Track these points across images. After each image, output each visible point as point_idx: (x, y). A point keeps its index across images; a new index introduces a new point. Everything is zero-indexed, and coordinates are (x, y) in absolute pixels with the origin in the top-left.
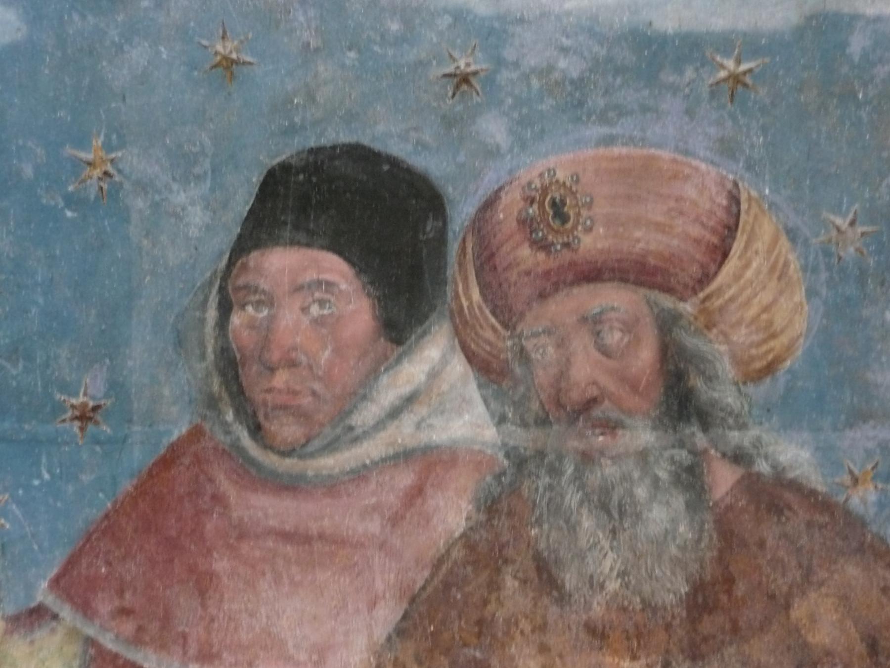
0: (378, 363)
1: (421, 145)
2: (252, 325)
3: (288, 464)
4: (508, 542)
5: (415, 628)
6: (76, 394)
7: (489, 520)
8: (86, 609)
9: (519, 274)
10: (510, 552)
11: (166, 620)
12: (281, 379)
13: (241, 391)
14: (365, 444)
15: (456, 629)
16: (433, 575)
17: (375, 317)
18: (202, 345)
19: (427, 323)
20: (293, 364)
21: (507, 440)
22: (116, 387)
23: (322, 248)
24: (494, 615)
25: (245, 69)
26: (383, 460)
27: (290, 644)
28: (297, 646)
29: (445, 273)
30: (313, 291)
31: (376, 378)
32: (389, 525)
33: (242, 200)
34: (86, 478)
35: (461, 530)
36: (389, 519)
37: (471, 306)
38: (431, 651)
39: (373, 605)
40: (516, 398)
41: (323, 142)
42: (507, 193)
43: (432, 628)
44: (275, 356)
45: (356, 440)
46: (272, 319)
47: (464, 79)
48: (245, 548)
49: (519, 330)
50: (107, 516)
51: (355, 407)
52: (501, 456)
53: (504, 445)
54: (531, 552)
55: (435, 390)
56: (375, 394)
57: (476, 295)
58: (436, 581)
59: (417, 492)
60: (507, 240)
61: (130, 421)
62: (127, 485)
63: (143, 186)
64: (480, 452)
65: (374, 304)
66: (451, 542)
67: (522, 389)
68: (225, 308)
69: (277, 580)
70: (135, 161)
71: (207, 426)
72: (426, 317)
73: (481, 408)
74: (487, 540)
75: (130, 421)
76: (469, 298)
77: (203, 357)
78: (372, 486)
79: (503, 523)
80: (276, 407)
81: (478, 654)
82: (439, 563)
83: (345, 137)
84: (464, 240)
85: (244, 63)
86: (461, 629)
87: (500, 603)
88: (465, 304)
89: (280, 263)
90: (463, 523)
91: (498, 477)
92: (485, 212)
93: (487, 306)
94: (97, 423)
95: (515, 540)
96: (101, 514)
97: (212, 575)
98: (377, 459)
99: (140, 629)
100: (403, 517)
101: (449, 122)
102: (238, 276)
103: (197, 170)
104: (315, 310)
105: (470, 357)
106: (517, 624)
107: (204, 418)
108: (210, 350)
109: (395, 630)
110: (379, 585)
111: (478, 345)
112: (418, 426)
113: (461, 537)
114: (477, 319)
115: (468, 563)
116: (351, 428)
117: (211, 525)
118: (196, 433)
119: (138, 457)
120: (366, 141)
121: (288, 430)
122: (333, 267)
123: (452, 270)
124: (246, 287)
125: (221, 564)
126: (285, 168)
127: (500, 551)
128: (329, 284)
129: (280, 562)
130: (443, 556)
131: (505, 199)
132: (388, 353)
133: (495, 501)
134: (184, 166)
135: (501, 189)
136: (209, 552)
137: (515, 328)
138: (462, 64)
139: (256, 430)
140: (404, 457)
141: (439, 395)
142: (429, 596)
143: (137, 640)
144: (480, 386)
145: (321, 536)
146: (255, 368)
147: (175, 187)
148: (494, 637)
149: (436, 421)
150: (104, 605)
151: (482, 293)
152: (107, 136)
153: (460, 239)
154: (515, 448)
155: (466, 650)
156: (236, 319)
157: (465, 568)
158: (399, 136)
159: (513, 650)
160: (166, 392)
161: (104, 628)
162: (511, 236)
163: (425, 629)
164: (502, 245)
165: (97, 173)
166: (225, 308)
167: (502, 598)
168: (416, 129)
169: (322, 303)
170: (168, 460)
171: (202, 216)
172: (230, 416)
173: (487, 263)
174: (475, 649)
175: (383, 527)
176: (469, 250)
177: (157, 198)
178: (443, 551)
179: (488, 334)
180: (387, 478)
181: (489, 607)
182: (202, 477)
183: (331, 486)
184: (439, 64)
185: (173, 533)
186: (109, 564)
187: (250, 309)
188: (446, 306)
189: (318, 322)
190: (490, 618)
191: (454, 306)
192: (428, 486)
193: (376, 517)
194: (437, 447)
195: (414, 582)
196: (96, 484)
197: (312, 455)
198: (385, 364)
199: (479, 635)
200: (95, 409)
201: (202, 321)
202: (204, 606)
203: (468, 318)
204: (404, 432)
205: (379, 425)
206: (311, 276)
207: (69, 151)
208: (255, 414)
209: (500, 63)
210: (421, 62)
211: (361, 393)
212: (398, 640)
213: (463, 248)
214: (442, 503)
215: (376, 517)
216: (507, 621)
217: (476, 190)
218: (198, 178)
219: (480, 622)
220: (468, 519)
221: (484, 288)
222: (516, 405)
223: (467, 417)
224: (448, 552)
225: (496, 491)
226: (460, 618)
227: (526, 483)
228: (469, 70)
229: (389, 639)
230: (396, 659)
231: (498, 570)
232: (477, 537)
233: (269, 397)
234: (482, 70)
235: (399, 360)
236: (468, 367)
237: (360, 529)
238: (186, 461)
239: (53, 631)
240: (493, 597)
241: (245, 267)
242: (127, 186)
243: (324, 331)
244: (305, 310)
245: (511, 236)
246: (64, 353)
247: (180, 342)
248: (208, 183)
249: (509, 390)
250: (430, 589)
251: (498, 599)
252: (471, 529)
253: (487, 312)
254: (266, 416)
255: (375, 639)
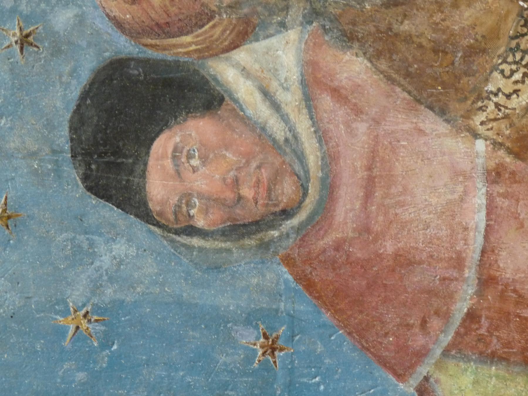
0: (237, 116)
1: (73, 73)
2: (205, 211)
3: (313, 191)
4: (375, 26)
5: (440, 101)
6: (255, 351)
7: (358, 40)
8: (421, 354)
9: (173, 6)
10: (383, 26)
11: (431, 292)
12: (247, 192)
13: (256, 223)
14: (299, 130)
15: (441, 70)
16: (400, 85)
17: (203, 116)
18: (219, 251)
19: (208, 77)
20: (236, 182)
21: (298, 22)
22: (250, 319)
23: (148, 153)
24: (430, 40)
25: (10, 203)
26: (311, 118)
27: (449, 197)
28: (453, 192)
29: (170, 62)
30: (180, 163)
31: (249, 119)
32: (361, 116)
33: (109, 212)
34: (320, 348)
35: (366, 61)
36: (356, 115)
37: (196, 44)
38: (456, 90)
39: (421, 132)
40: (267, 14)
41: (67, 147)
42: (112, 11)
43: (440, 88)
44: (229, 195)
45: (296, 137)
46: (200, 196)
47: (25, 41)
48: (377, 228)
49: (215, 9)
50: (350, 334)
51: (270, 136)
52: (309, 28)
53: (302, 24)
54: (383, 10)
55: (259, 74)
56: (260, 120)
57: (188, 39)
58: (403, 82)
59: (336, 93)
60: (148, 14)
61: (277, 310)
62: (326, 317)
63: (96, 288)
64: (306, 43)
65: (192, 116)
66: (374, 70)
67: (259, 9)
68: (191, 231)
69: (401, 204)
70: (76, 295)
71: (282, 252)
72: (203, 77)
73: (273, 40)
74: (373, 42)
75: (277, 310)
76: (190, 44)
77: (228, 251)
78: (331, 127)
79: (360, 30)
80: (269, 198)
81: (460, 55)
82: (389, 79)
83: (65, 131)
84: (146, 45)
85: (6, 204)
86: (441, 65)
87: (421, 35)
88: (194, 47)
89: (159, 186)
90: (360, 59)
91: (326, 31)
92: (124, 28)
93: (197, 31)
94: (277, 338)
95: (374, 21)
96: (348, 338)
97: (397, 255)
98: (311, 122)
99: (437, 313)
100: (355, 105)
101: (56, 52)
102: (168, 220)
103: (85, 246)
104: (195, 162)
105: (234, 46)
106: (437, 24)
107: (276, 253)
108: (223, 245)
109: (441, 117)
110: (407, 126)
111: (225, 40)
112: (287, 89)
113: (371, 62)
114: (205, 39)
115: (390, 58)
116: (287, 140)
117: (358, 253)
118: (288, 261)
119: (304, 306)
120: (68, 116)
121: (287, 190)
122: (163, 145)
123: (168, 56)
124: (175, 214)
125: (389, 247)
126: (85, 178)
127: (381, 33)
128: (175, 150)
129: (387, 201)
130: (385, 76)
131: (116, 13)
132: (230, 108)
133: (344, 34)
134: (82, 255)
135: (108, 15)
136: (379, 255)
137: (214, 11)
138: (14, 39)
139: (286, 213)
140: (309, 101)
141: (262, 71)
142: (416, 89)
143: (446, 316)
144: (257, 40)
145: (369, 169)
146: (238, 211)
147: (97, 264)
148: (446, 41)
149: (283, 75)
150: (419, 341)
151: (187, 34)
152: (57, 313)
153: (145, 49)
154: (304, 17)
155: (457, 64)
156: (200, 223)
157: (395, 60)
158: (65, 90)
159: (456, 28)
160: (255, 281)
161: (436, 341)
162: (143, 9)
163: (441, 93)
164: (150, 17)
165: (84, 324)
166: (191, 231)
167: (417, 34)
168: (61, 76)
169: (190, 157)
170: (309, 285)
171: (121, 246)
172: (275, 233)
173: (163, 29)
174: (456, 57)
175: (362, 121)
176: (153, 42)
177: (105, 278)
178: (382, 76)
179: (218, 31)
180: (325, 115)
181: (424, 43)
182: (322, 258)
183: (330, 159)
184: (13, 56)
185: (364, 283)
186: (386, 335)
187: (192, 212)
188: (195, 62)
189: (204, 159)
190: (432, 44)
191: (196, 56)
192: (332, 84)
193: (354, 125)
194: (302, 75)
195: (404, 99)
196: (324, 342)
197: (307, 172)
198: (238, 110)
199: (445, 53)
200: (266, 337)
201: (201, 249)
202: (420, 263)
203: (204, 46)
204: (290, 99)
205: (285, 118)
206: (169, 163)
207: (67, 343)
208: (274, 214)
209: (14, 11)
210: (11, 70)
211: (260, 131)
212: (448, 115)
213: (152, 46)
214: (345, 75)
215: (354, 125)
216: (435, 31)
217: (109, 34)
218: (92, 245)
219: (435, 51)
220: (357, 55)
221: (182, 33)
222: (272, 13)
223: (280, 53)
224: (382, 72)
225: (336, 33)
226: (432, 66)
227: (331, 10)
228: (18, 34)
229: (448, 121)
230: (462, 116)
231: (397, 35)
232: (371, 50)
233: (261, 202)
234: (19, 24)
235: (236, 101)
236: (241, 48)
237: (364, 138)
238: (309, 270)
239: (437, 381)
240: (415, 39)
241: (161, 214)
242: (95, 300)
243: (211, 156)
244: (195, 170)
245: (143, 9)
246: (223, 359)
247: (217, 268)
248: (96, 238)
249: (260, 18)
250: (410, 88)
251: (417, 37)
252: (365, 54)
253: (200, 31)
254: (275, 205)
255: (447, 131)
